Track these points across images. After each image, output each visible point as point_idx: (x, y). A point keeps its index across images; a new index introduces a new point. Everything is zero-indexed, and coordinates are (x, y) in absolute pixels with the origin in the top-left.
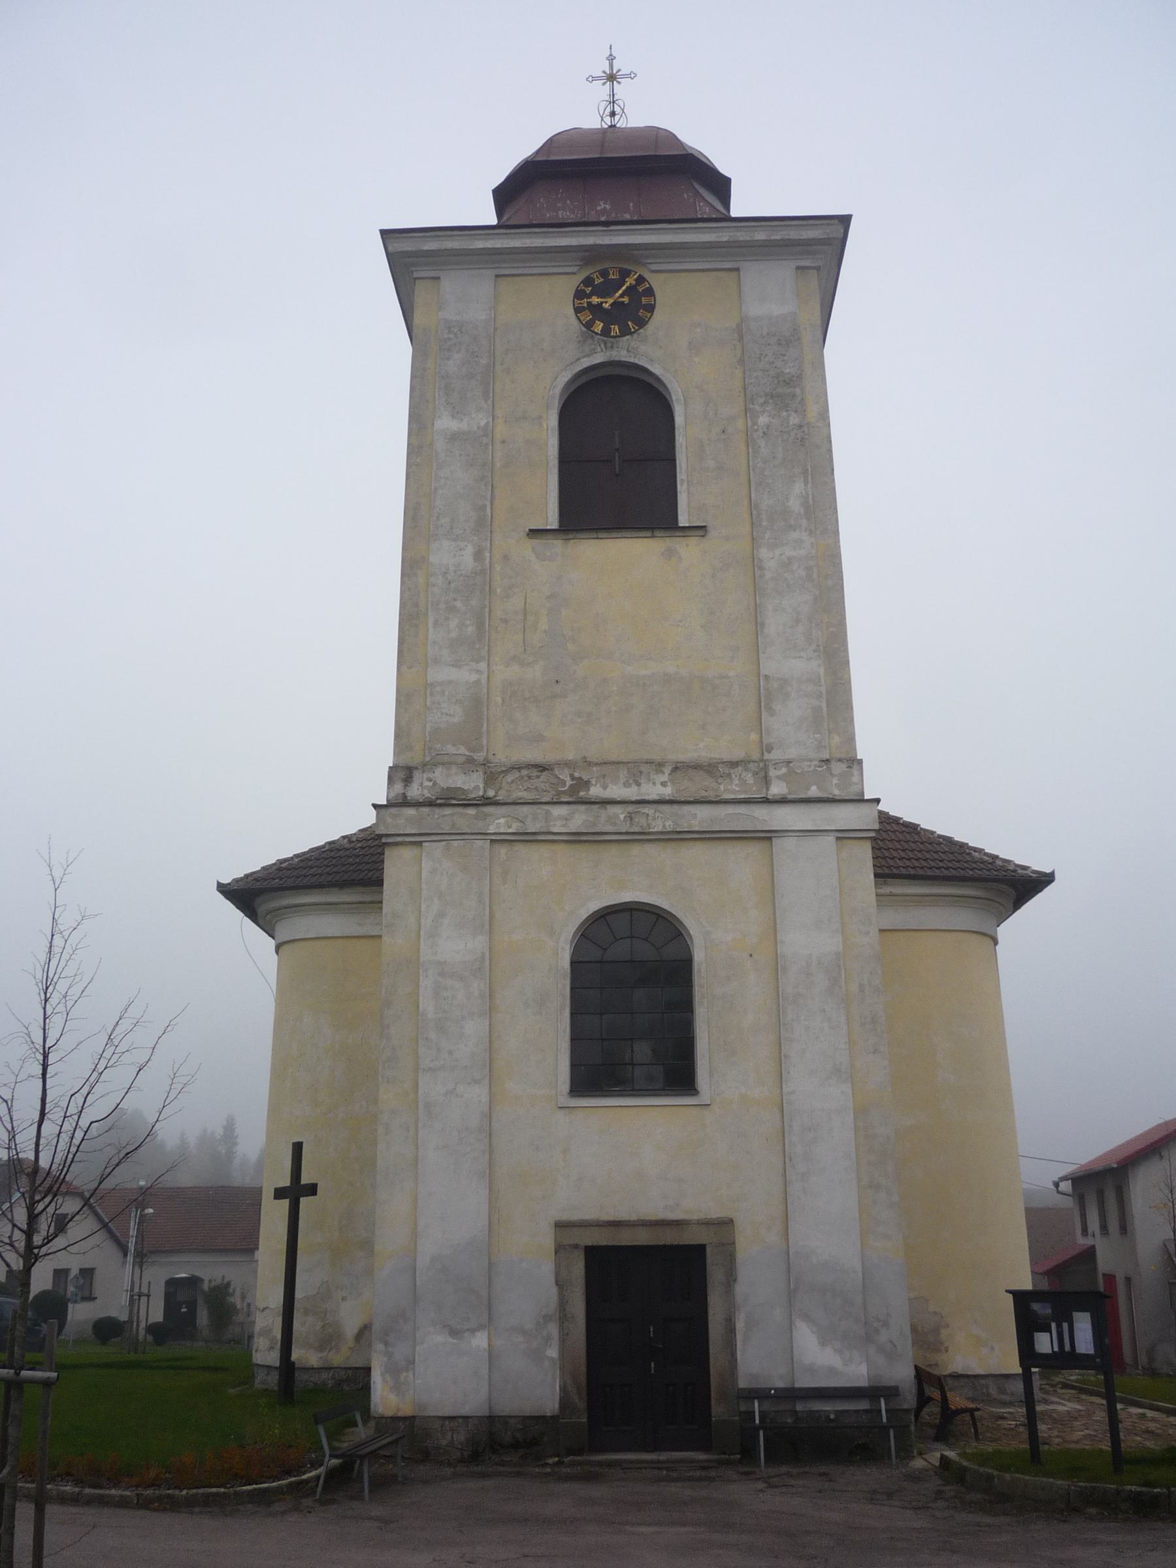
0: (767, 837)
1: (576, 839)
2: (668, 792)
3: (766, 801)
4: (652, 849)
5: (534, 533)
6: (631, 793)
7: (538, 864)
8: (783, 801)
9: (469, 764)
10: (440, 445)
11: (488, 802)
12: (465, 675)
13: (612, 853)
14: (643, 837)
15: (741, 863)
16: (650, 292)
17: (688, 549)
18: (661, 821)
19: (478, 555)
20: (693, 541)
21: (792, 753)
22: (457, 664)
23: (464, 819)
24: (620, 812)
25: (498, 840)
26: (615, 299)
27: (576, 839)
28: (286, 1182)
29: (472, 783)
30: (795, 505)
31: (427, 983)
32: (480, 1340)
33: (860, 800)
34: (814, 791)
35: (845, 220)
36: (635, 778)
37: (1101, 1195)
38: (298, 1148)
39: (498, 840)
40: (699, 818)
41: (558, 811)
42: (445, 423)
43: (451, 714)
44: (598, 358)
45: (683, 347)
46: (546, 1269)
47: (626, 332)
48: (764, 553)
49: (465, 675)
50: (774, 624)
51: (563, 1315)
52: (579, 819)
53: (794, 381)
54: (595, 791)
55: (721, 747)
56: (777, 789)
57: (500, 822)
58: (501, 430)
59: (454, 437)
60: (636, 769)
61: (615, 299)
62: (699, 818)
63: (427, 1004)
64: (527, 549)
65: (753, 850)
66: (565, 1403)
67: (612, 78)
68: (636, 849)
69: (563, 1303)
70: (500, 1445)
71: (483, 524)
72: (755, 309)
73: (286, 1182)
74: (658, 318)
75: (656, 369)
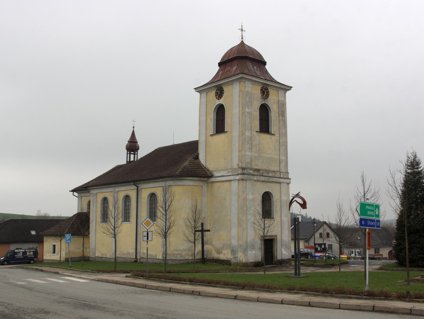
0: (280, 183)
1: (263, 181)
5: (257, 132)
7: (259, 185)
8: (282, 178)
10: (246, 113)
11: (254, 175)
12: (250, 154)
17: (273, 137)
18: (271, 179)
22: (249, 152)
23: (251, 177)
24: (267, 178)
25: (255, 181)
26: (265, 92)
29: (251, 172)
30: (284, 132)
31: (248, 202)
32: (254, 252)
33: (288, 179)
34: (285, 177)
35: (292, 87)
39: (255, 181)
40: (275, 180)
41: (262, 177)
42: (247, 110)
43: (248, 160)
46: (260, 242)
47: (266, 98)
48: (281, 140)
49: (250, 154)
51: (261, 248)
52: (263, 178)
54: (264, 174)
55: (276, 169)
56: (282, 176)
57: (255, 178)
59: (248, 112)
61: (265, 92)
62: (275, 180)
63: (248, 205)
64: (256, 134)
65: (279, 184)
66: (261, 259)
68: (268, 183)
69: (261, 246)
70: (257, 265)
71: (251, 129)
72: (280, 99)
74: (270, 97)
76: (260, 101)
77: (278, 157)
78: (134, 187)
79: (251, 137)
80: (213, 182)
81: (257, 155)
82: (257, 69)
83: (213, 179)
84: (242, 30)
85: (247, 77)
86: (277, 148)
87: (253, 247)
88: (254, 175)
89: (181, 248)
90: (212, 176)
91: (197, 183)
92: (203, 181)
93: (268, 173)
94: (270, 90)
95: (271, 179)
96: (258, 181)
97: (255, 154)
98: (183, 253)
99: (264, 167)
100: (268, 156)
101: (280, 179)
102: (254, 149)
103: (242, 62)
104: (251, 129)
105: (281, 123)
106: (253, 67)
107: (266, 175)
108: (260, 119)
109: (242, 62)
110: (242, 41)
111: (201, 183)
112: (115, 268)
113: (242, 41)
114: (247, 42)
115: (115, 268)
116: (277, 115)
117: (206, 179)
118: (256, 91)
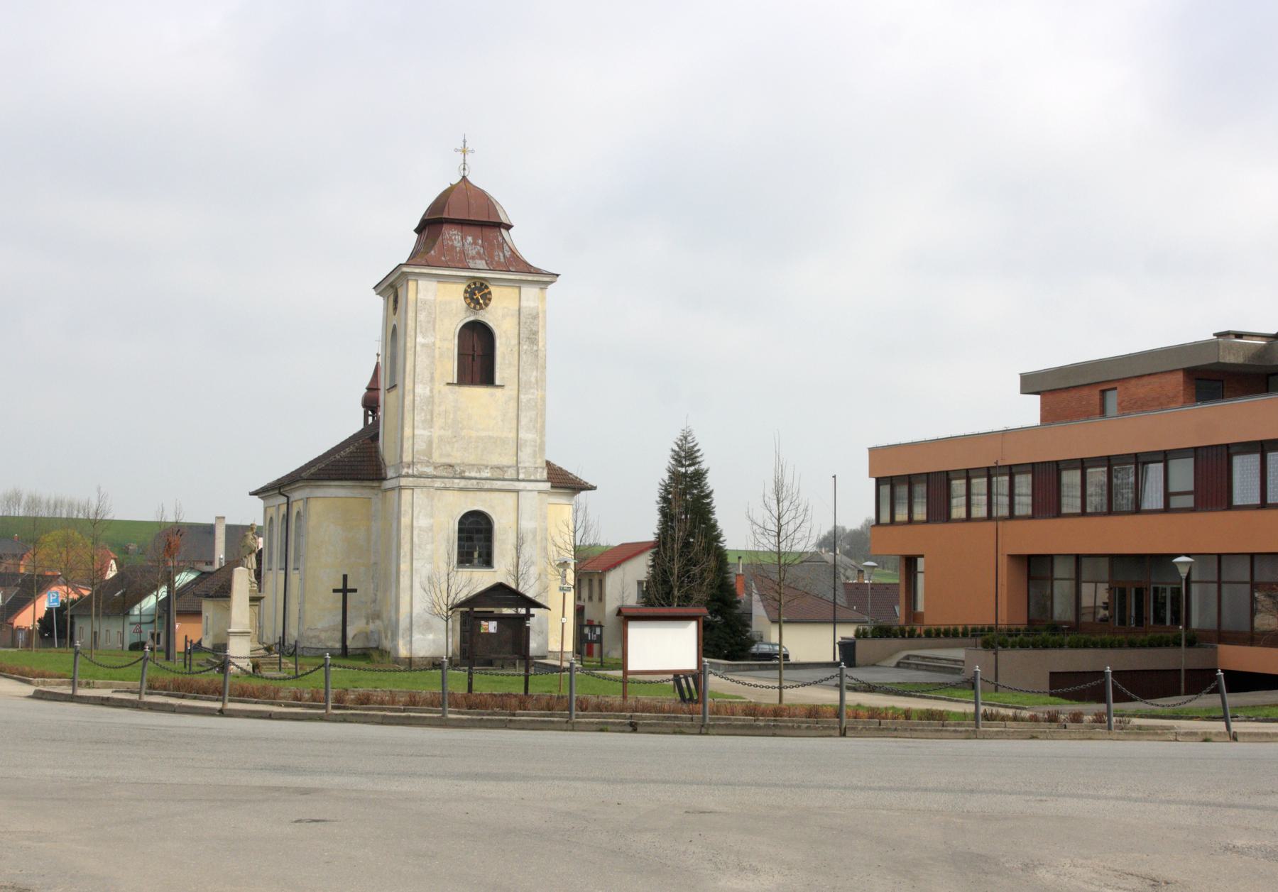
0: (517, 491)
1: (461, 489)
2: (489, 475)
3: (518, 480)
4: (483, 493)
6: (478, 475)
7: (450, 496)
9: (428, 463)
11: (436, 477)
12: (426, 433)
13: (471, 494)
16: (490, 293)
18: (487, 485)
19: (431, 391)
20: (500, 390)
21: (527, 465)
25: (438, 489)
26: (478, 294)
27: (461, 489)
28: (341, 587)
29: (430, 470)
30: (533, 380)
32: (431, 636)
36: (479, 471)
37: (591, 581)
38: (345, 577)
39: (438, 489)
40: (498, 484)
44: (472, 318)
48: (522, 396)
49: (426, 433)
50: (524, 421)
52: (462, 483)
53: (536, 333)
54: (467, 474)
56: (521, 476)
57: (438, 483)
59: (423, 345)
60: (479, 468)
61: (478, 294)
62: (498, 484)
63: (415, 539)
65: (514, 495)
67: (464, 152)
71: (432, 379)
73: (341, 587)
74: (492, 304)
75: (491, 324)
76: (462, 315)
77: (513, 435)
78: (285, 499)
79: (432, 397)
82: (475, 243)
83: (387, 484)
84: (464, 152)
85: (417, 270)
86: (512, 414)
87: (428, 627)
88: (436, 477)
89: (319, 626)
90: (385, 479)
91: (357, 492)
92: (373, 488)
93: (479, 471)
94: (492, 289)
95: (487, 485)
96: (446, 489)
97: (442, 433)
98: (323, 635)
99: (472, 459)
100: (484, 434)
101: (517, 484)
102: (439, 422)
103: (460, 226)
104: (432, 379)
105: (524, 357)
107: (473, 474)
108: (460, 355)
109: (460, 226)
110: (464, 177)
111: (367, 493)
112: (624, 697)
113: (464, 177)
114: (475, 180)
115: (624, 697)
116: (515, 342)
117: (376, 484)
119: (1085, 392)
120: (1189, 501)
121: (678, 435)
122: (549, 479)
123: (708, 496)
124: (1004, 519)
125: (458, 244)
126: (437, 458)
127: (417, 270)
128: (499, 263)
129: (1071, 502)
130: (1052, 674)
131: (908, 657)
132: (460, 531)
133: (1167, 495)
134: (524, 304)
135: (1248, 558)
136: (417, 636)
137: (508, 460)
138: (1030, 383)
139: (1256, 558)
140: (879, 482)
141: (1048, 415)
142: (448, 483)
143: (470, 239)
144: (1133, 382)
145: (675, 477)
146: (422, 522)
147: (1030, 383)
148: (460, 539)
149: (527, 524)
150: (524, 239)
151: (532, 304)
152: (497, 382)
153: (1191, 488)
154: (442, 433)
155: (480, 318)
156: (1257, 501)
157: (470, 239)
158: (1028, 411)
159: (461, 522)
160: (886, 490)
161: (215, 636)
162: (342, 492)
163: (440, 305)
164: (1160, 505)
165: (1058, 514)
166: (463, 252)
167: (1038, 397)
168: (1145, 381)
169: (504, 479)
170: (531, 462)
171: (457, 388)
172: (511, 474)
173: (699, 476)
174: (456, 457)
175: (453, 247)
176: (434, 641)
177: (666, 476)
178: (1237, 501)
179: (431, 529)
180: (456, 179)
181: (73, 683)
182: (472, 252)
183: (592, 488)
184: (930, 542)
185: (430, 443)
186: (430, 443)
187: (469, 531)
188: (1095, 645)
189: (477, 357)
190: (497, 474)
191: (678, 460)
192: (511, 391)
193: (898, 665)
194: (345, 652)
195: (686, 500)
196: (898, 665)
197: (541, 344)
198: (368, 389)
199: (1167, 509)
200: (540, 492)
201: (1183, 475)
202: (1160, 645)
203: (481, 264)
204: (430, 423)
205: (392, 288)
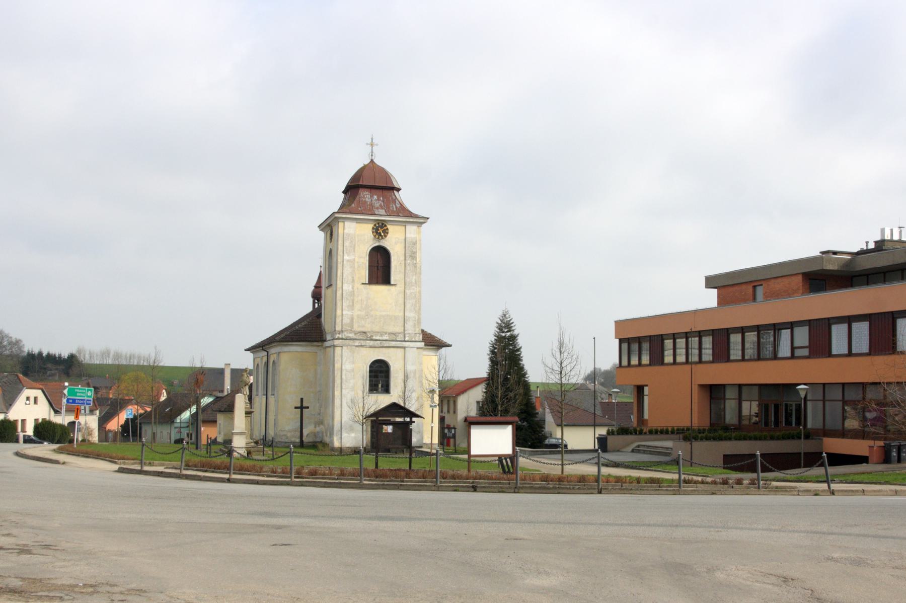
0: (404, 348)
1: (371, 347)
9: (351, 331)
12: (350, 313)
13: (377, 350)
14: (383, 347)
15: (400, 352)
18: (387, 344)
23: (351, 342)
26: (380, 229)
27: (371, 347)
29: (352, 335)
32: (353, 435)
36: (381, 335)
37: (448, 401)
38: (302, 400)
40: (393, 344)
44: (377, 244)
45: (394, 242)
48: (407, 291)
49: (350, 313)
50: (408, 306)
52: (372, 343)
53: (415, 253)
57: (357, 343)
58: (357, 259)
59: (348, 261)
60: (382, 334)
61: (380, 229)
62: (393, 344)
65: (402, 350)
71: (353, 281)
74: (389, 235)
75: (388, 248)
76: (371, 243)
77: (402, 314)
80: (326, 348)
81: (363, 313)
82: (378, 199)
83: (327, 344)
84: (372, 145)
85: (344, 216)
86: (401, 300)
87: (351, 429)
89: (287, 429)
90: (325, 341)
93: (381, 335)
94: (389, 226)
95: (387, 344)
96: (362, 346)
97: (359, 313)
98: (289, 434)
99: (376, 329)
100: (384, 313)
102: (357, 307)
103: (369, 189)
104: (353, 281)
105: (408, 268)
106: (372, 196)
107: (378, 338)
109: (369, 189)
111: (314, 349)
112: (469, 471)
114: (379, 162)
115: (469, 471)
116: (402, 258)
117: (320, 344)
118: (366, 230)
119: (744, 287)
120: (806, 352)
121: (500, 313)
122: (423, 340)
123: (519, 350)
124: (696, 363)
125: (368, 200)
126: (356, 328)
127: (344, 216)
128: (393, 211)
129: (736, 353)
130: (725, 456)
131: (638, 446)
132: (370, 371)
133: (793, 349)
134: (408, 235)
135: (841, 386)
136: (345, 435)
137: (399, 329)
138: (711, 282)
139: (846, 387)
140: (621, 341)
141: (722, 301)
142: (363, 343)
143: (375, 197)
144: (773, 281)
145: (499, 339)
146: (347, 366)
147: (711, 282)
148: (370, 376)
149: (410, 368)
150: (407, 197)
151: (413, 236)
152: (392, 282)
153: (807, 344)
154: (359, 313)
155: (382, 244)
156: (846, 352)
157: (375, 197)
158: (710, 299)
159: (371, 366)
160: (625, 346)
161: (225, 435)
162: (299, 349)
163: (357, 237)
164: (789, 355)
165: (728, 360)
166: (371, 205)
167: (716, 290)
168: (779, 280)
169: (397, 340)
170: (412, 330)
171: (368, 286)
172: (400, 337)
173: (513, 338)
174: (368, 327)
175: (366, 202)
176: (355, 438)
177: (493, 338)
178: (834, 352)
179: (353, 370)
180: (367, 162)
181: (141, 463)
182: (377, 205)
183: (449, 346)
184: (651, 377)
185: (352, 319)
186: (352, 319)
187: (376, 372)
188: (750, 439)
189: (380, 267)
190: (393, 337)
191: (500, 328)
192: (400, 288)
193: (633, 451)
194: (302, 445)
195: (506, 353)
196: (633, 451)
197: (418, 259)
198: (315, 287)
199: (793, 357)
200: (418, 348)
201: (802, 336)
202: (788, 438)
203: (382, 212)
204: (352, 307)
205: (329, 227)
